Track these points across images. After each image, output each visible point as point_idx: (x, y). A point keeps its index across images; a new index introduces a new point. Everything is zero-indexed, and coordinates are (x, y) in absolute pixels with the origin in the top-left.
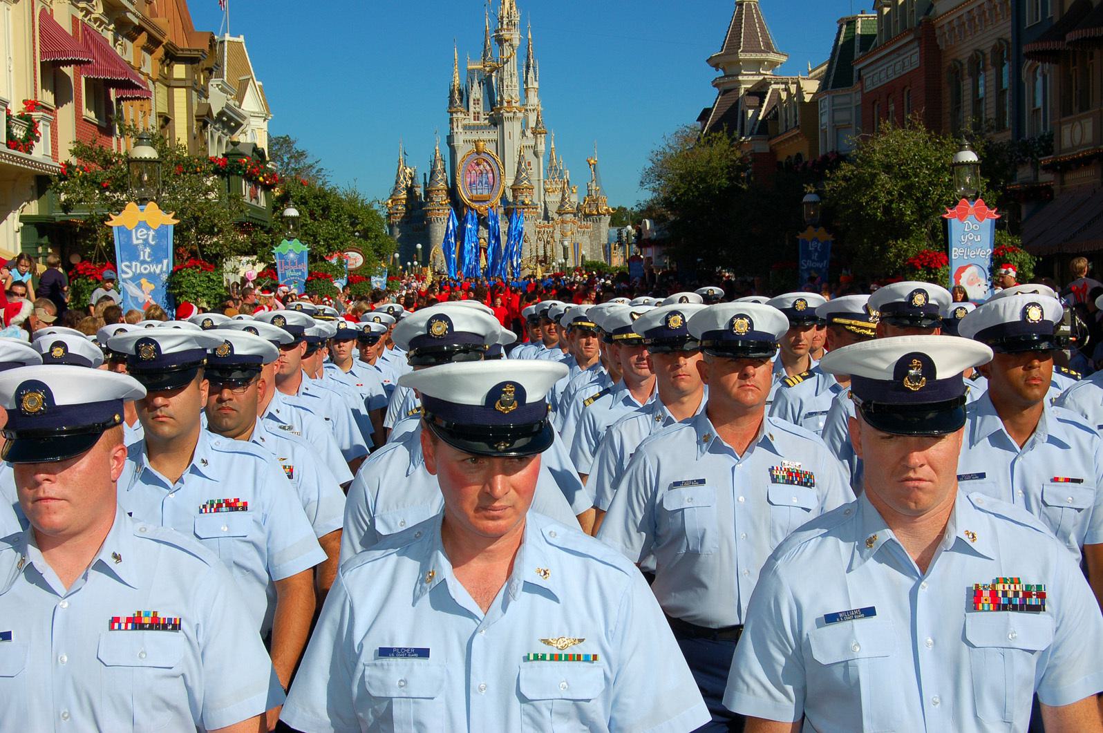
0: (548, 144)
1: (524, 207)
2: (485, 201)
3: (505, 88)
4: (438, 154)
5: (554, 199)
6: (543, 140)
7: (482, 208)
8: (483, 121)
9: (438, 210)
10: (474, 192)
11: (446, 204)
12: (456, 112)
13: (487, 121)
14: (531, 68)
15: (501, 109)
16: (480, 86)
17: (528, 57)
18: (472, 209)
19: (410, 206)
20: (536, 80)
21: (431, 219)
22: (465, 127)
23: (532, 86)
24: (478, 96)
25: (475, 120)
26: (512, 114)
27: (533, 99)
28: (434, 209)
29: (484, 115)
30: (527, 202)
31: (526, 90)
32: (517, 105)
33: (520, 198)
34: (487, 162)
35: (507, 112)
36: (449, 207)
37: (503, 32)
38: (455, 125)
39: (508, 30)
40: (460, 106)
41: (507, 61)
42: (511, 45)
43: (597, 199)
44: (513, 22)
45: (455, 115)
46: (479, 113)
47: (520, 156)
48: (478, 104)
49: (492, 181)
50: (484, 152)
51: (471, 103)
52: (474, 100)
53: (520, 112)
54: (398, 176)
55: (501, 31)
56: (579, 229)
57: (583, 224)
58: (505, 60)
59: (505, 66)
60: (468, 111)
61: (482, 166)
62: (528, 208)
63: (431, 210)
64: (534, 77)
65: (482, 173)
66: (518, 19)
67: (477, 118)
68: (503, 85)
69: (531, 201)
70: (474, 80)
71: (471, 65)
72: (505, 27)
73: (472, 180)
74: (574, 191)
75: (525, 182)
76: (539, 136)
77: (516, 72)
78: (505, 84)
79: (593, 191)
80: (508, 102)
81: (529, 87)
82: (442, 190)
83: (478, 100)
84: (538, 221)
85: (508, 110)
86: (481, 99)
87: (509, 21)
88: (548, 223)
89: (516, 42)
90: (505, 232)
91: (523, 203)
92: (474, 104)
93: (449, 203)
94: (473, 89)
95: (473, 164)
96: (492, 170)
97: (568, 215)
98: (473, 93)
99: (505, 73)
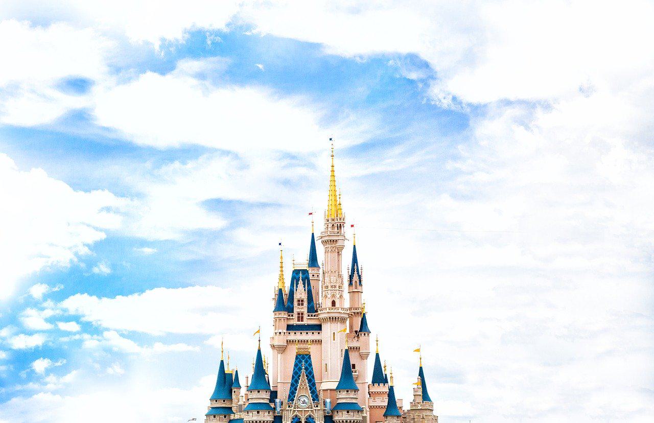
16: (304, 287)
25: (298, 321)
29: (309, 316)
46: (302, 314)
51: (296, 303)
52: (299, 301)
64: (358, 282)
83: (302, 301)
92: (299, 305)
94: (298, 289)
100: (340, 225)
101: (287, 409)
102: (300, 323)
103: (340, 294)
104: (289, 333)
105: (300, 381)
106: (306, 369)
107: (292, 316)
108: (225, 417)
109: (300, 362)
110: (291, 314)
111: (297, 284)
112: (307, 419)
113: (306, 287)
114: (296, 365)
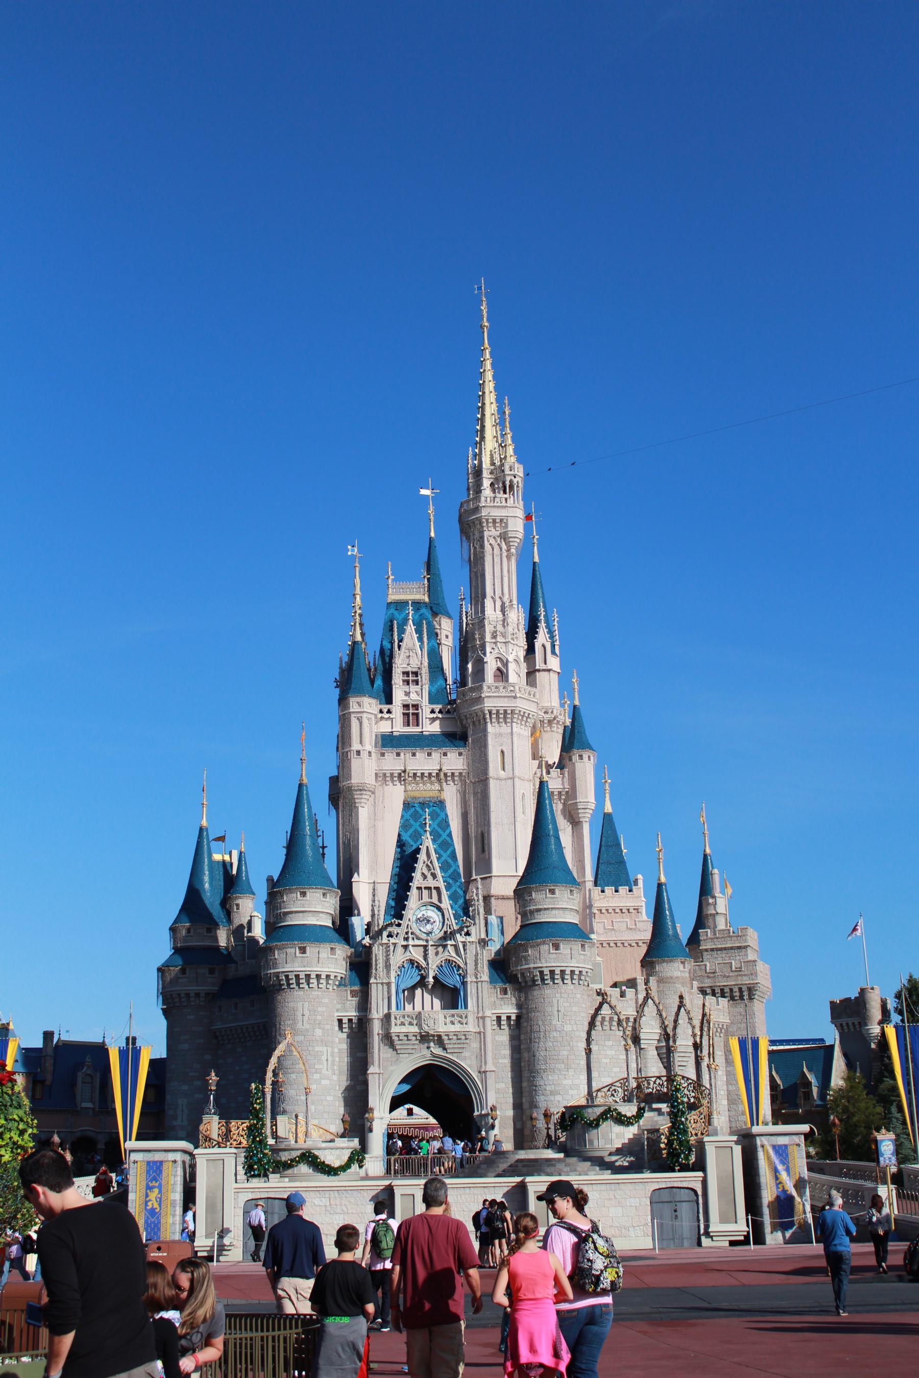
3: (488, 638)
14: (542, 625)
16: (420, 639)
20: (553, 652)
22: (389, 741)
23: (543, 667)
24: (414, 664)
29: (433, 712)
44: (508, 479)
48: (417, 683)
51: (397, 679)
60: (389, 700)
67: (411, 714)
78: (489, 629)
87: (496, 479)
90: (499, 1018)
94: (403, 644)
99: (488, 603)
100: (511, 481)
101: (386, 941)
102: (413, 730)
104: (383, 755)
105: (420, 867)
106: (436, 836)
107: (389, 712)
108: (212, 971)
109: (416, 816)
110: (385, 708)
111: (402, 631)
112: (440, 967)
113: (425, 639)
114: (405, 826)
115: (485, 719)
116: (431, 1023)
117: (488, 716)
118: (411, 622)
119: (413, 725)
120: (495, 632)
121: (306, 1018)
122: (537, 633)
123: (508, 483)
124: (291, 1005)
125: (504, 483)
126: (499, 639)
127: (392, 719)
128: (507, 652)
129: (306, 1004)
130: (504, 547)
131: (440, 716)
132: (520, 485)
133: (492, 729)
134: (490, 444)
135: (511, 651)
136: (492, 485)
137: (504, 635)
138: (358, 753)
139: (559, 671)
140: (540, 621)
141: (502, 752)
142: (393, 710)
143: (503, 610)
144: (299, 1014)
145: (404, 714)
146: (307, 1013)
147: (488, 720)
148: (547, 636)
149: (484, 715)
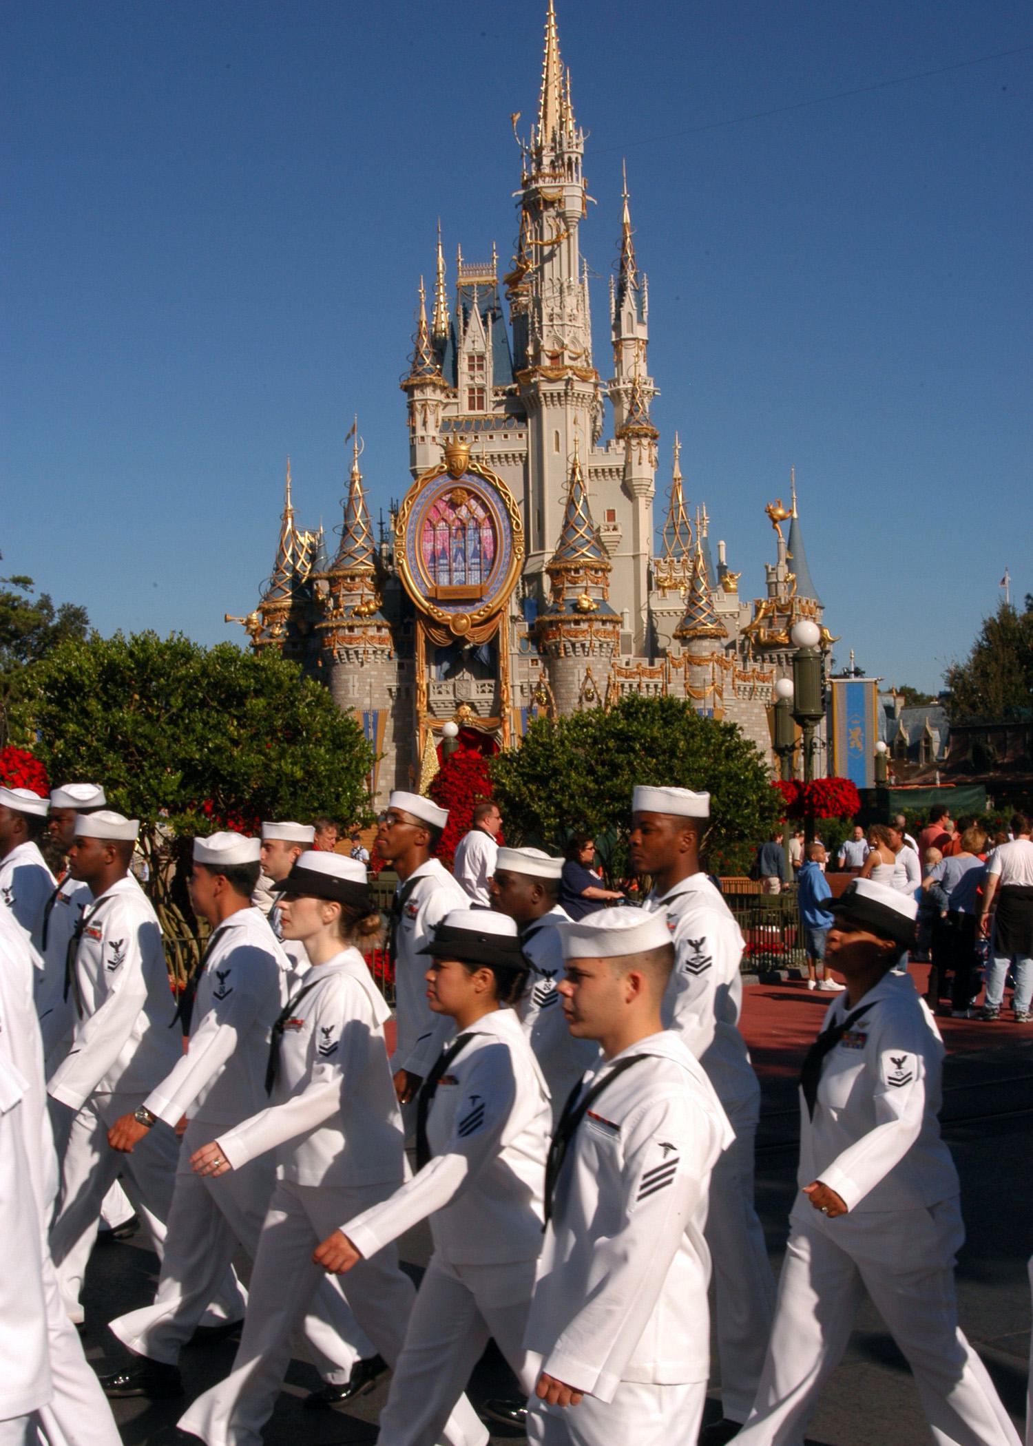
0: (662, 464)
1: (577, 617)
2: (470, 602)
3: (545, 321)
4: (357, 485)
5: (673, 603)
6: (645, 454)
7: (462, 619)
8: (493, 409)
9: (351, 629)
10: (444, 579)
11: (372, 613)
12: (422, 386)
13: (501, 411)
14: (630, 295)
15: (534, 372)
16: (485, 323)
17: (623, 268)
18: (437, 625)
19: (303, 627)
20: (640, 321)
21: (331, 651)
23: (630, 336)
24: (480, 347)
25: (472, 407)
26: (560, 386)
27: (635, 365)
28: (338, 627)
29: (497, 395)
30: (585, 604)
31: (617, 345)
32: (579, 364)
33: (569, 596)
34: (477, 498)
35: (550, 381)
36: (380, 619)
37: (541, 184)
38: (419, 418)
39: (555, 177)
40: (432, 372)
41: (552, 255)
42: (561, 215)
43: (790, 605)
44: (566, 157)
45: (418, 395)
47: (572, 483)
49: (489, 548)
50: (470, 472)
51: (463, 365)
52: (471, 358)
53: (584, 380)
54: (281, 555)
55: (537, 181)
56: (738, 682)
57: (749, 669)
58: (547, 250)
59: (547, 266)
60: (456, 385)
61: (463, 512)
62: (590, 620)
63: (332, 628)
64: (635, 314)
65: (463, 528)
66: (581, 150)
67: (477, 398)
68: (540, 322)
69: (602, 603)
70: (472, 307)
71: (468, 276)
72: (547, 170)
73: (439, 547)
74: (732, 586)
75: (584, 550)
76: (634, 442)
77: (574, 280)
78: (546, 311)
79: (781, 587)
80: (555, 357)
81: (625, 335)
82: (362, 576)
83: (481, 358)
84: (624, 658)
85: (551, 374)
86: (488, 356)
87: (557, 157)
88: (652, 664)
89: (575, 206)
91: (576, 607)
92: (471, 367)
93: (381, 609)
95: (442, 506)
96: (490, 519)
97: (706, 643)
98: (468, 341)
99: (547, 284)
100: (570, 159)
103: (571, 335)
107: (455, 396)
113: (490, 323)
115: (540, 402)
116: (463, 692)
117: (543, 399)
118: (476, 306)
119: (479, 409)
120: (552, 315)
121: (356, 688)
122: (623, 301)
123: (566, 160)
124: (344, 677)
125: (563, 160)
126: (555, 322)
127: (457, 404)
128: (563, 336)
129: (356, 676)
130: (563, 227)
131: (504, 398)
132: (580, 161)
133: (547, 412)
134: (553, 120)
135: (567, 333)
136: (552, 162)
137: (561, 317)
138: (423, 438)
139: (646, 338)
140: (626, 289)
141: (557, 433)
142: (459, 394)
143: (561, 292)
144: (350, 684)
145: (470, 398)
146: (357, 684)
147: (543, 403)
148: (633, 303)
149: (539, 398)
